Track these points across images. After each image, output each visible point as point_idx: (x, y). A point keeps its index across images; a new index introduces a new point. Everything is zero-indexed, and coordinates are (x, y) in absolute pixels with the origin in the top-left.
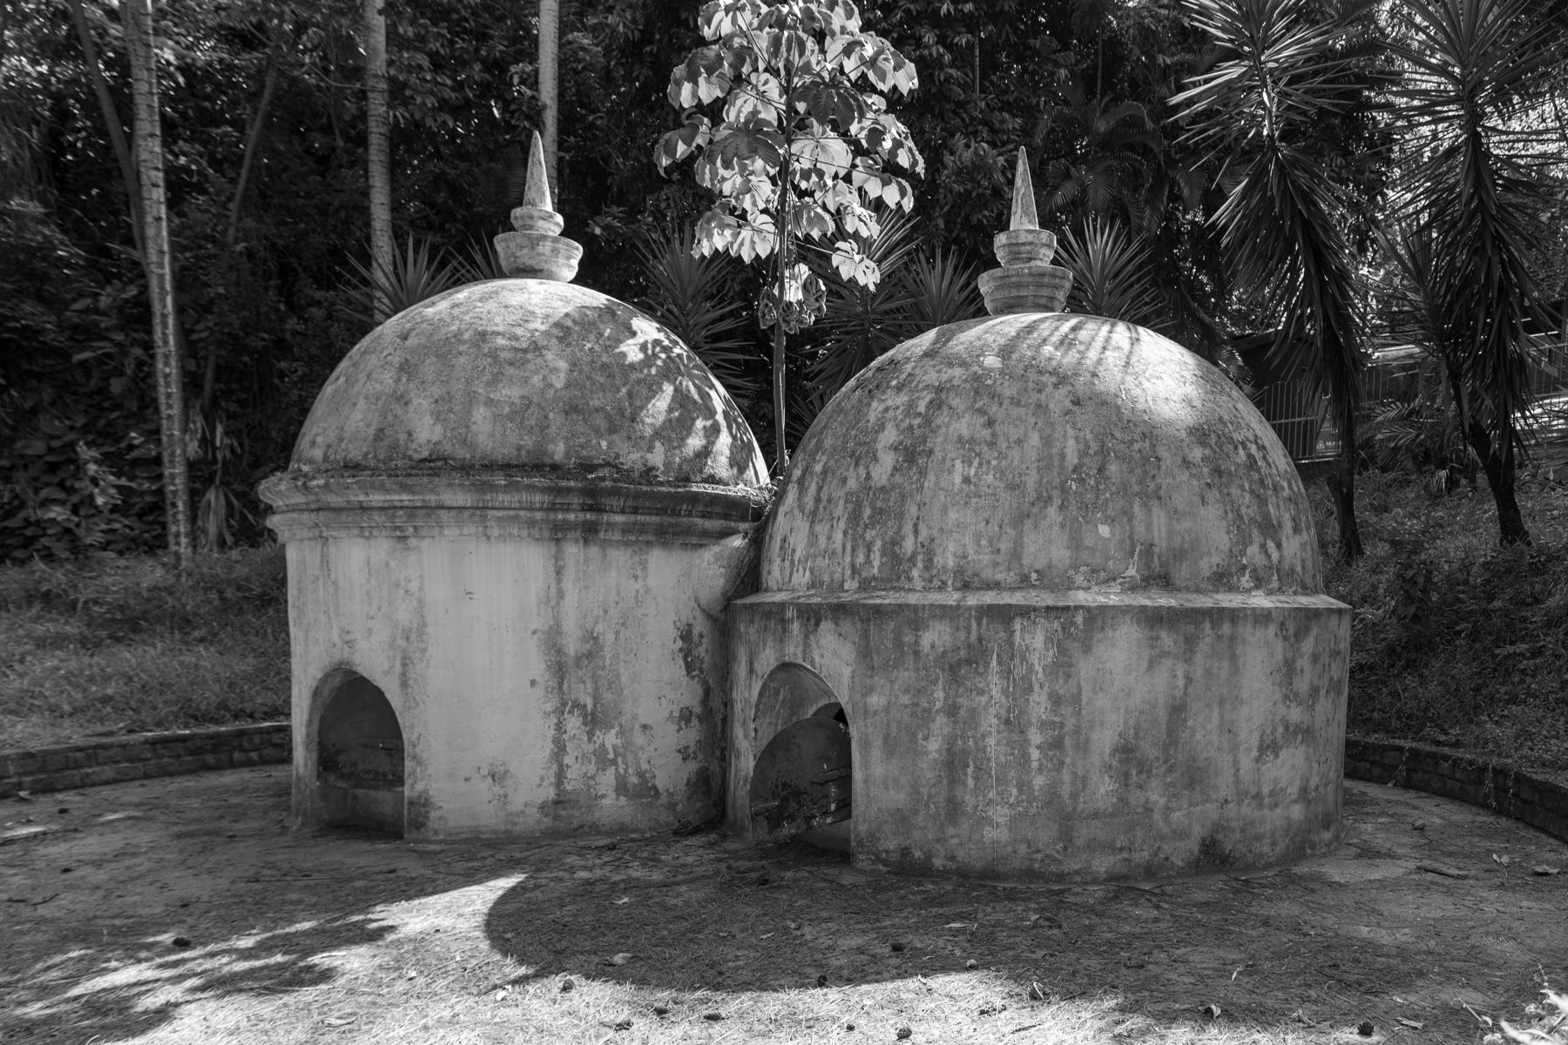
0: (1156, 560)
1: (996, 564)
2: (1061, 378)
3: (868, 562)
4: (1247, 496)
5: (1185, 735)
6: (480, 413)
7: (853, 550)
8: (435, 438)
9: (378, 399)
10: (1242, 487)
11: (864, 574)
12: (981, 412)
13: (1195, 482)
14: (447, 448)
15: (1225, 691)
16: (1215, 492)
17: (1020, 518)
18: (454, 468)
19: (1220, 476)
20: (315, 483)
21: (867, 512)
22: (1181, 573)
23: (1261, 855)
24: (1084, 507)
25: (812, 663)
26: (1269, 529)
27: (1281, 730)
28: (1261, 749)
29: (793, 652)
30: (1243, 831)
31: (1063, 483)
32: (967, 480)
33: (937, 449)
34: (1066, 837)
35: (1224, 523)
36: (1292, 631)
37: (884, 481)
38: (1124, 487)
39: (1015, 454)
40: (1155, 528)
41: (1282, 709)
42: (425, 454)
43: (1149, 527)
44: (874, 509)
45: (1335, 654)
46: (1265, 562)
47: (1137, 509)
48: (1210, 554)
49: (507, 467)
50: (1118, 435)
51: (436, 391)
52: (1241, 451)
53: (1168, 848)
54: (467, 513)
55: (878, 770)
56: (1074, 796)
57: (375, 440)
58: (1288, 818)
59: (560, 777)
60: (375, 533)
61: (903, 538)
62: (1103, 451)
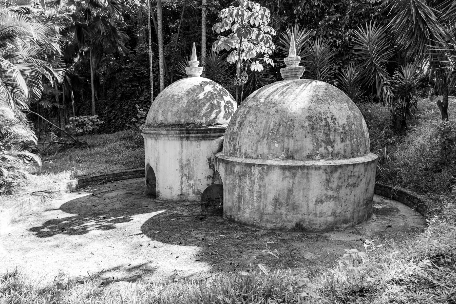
1: (252, 152)
2: (275, 105)
4: (322, 134)
5: (292, 197)
6: (170, 114)
12: (255, 114)
13: (304, 132)
14: (163, 122)
15: (305, 187)
16: (310, 134)
17: (258, 141)
22: (297, 156)
23: (315, 229)
24: (272, 139)
30: (309, 222)
31: (268, 133)
32: (249, 132)
34: (261, 218)
35: (312, 142)
39: (260, 125)
42: (160, 123)
43: (288, 144)
48: (306, 151)
50: (284, 120)
51: (163, 109)
53: (286, 224)
56: (263, 209)
59: (182, 189)
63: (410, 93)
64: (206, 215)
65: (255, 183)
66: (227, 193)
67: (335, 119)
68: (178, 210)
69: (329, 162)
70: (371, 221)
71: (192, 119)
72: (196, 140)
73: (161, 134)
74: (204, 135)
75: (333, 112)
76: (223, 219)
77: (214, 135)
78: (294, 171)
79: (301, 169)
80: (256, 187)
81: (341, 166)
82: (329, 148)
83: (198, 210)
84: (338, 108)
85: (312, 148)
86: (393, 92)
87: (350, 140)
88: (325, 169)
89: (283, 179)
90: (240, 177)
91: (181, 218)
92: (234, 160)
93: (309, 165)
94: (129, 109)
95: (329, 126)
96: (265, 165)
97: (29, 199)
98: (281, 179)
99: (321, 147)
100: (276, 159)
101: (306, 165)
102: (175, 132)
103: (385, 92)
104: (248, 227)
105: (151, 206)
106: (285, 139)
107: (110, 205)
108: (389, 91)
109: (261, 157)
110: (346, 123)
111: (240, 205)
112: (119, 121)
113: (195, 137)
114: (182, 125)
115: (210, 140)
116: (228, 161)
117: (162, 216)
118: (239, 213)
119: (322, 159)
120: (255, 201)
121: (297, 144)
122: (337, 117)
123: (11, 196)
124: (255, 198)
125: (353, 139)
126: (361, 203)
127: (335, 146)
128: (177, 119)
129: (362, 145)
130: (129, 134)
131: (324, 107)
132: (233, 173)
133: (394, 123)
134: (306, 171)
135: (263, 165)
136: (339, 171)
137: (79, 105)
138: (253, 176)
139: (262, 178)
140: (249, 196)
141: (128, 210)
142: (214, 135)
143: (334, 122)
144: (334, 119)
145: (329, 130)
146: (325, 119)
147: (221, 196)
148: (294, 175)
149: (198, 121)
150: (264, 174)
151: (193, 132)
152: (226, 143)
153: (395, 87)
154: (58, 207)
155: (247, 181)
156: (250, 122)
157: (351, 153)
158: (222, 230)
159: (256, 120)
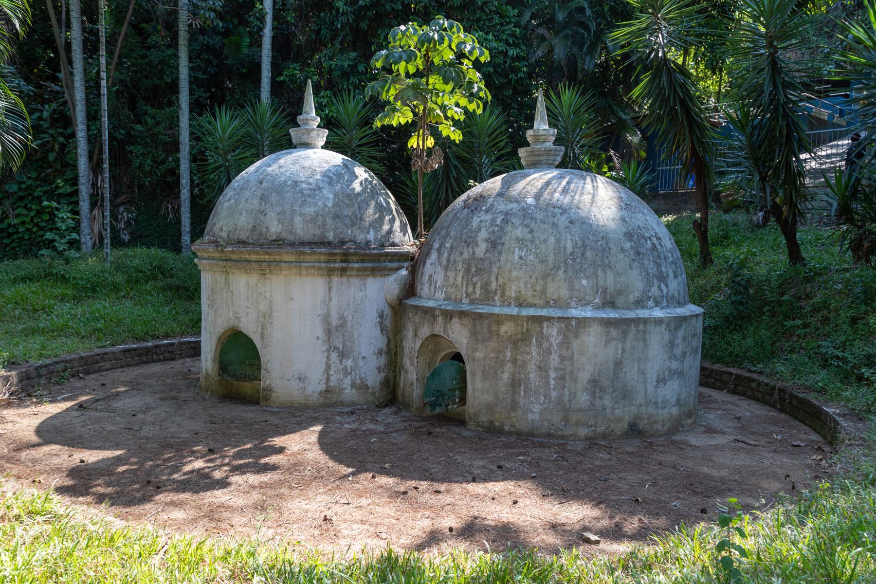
3: (474, 292)
4: (652, 264)
6: (298, 219)
7: (467, 286)
8: (279, 231)
9: (252, 212)
10: (649, 260)
11: (472, 297)
13: (627, 259)
14: (284, 235)
16: (636, 263)
18: (288, 245)
19: (639, 255)
20: (227, 249)
21: (474, 269)
25: (448, 336)
26: (662, 278)
29: (438, 329)
33: (506, 243)
35: (641, 277)
36: (673, 327)
37: (481, 256)
41: (668, 363)
42: (274, 238)
44: (477, 268)
45: (694, 335)
46: (660, 294)
49: (310, 244)
51: (278, 209)
52: (649, 242)
54: (293, 264)
57: (252, 231)
60: (252, 272)
61: (491, 282)
71: (349, 232)
72: (358, 276)
74: (376, 265)
78: (625, 327)
79: (635, 325)
89: (606, 343)
90: (515, 343)
96: (572, 318)
98: (603, 343)
106: (600, 272)
109: (558, 303)
111: (517, 397)
113: (359, 270)
114: (329, 243)
115: (382, 275)
120: (552, 387)
121: (619, 280)
124: (552, 382)
128: (318, 232)
132: (495, 338)
135: (568, 318)
138: (547, 340)
139: (565, 344)
148: (625, 334)
149: (361, 237)
151: (355, 258)
155: (534, 350)
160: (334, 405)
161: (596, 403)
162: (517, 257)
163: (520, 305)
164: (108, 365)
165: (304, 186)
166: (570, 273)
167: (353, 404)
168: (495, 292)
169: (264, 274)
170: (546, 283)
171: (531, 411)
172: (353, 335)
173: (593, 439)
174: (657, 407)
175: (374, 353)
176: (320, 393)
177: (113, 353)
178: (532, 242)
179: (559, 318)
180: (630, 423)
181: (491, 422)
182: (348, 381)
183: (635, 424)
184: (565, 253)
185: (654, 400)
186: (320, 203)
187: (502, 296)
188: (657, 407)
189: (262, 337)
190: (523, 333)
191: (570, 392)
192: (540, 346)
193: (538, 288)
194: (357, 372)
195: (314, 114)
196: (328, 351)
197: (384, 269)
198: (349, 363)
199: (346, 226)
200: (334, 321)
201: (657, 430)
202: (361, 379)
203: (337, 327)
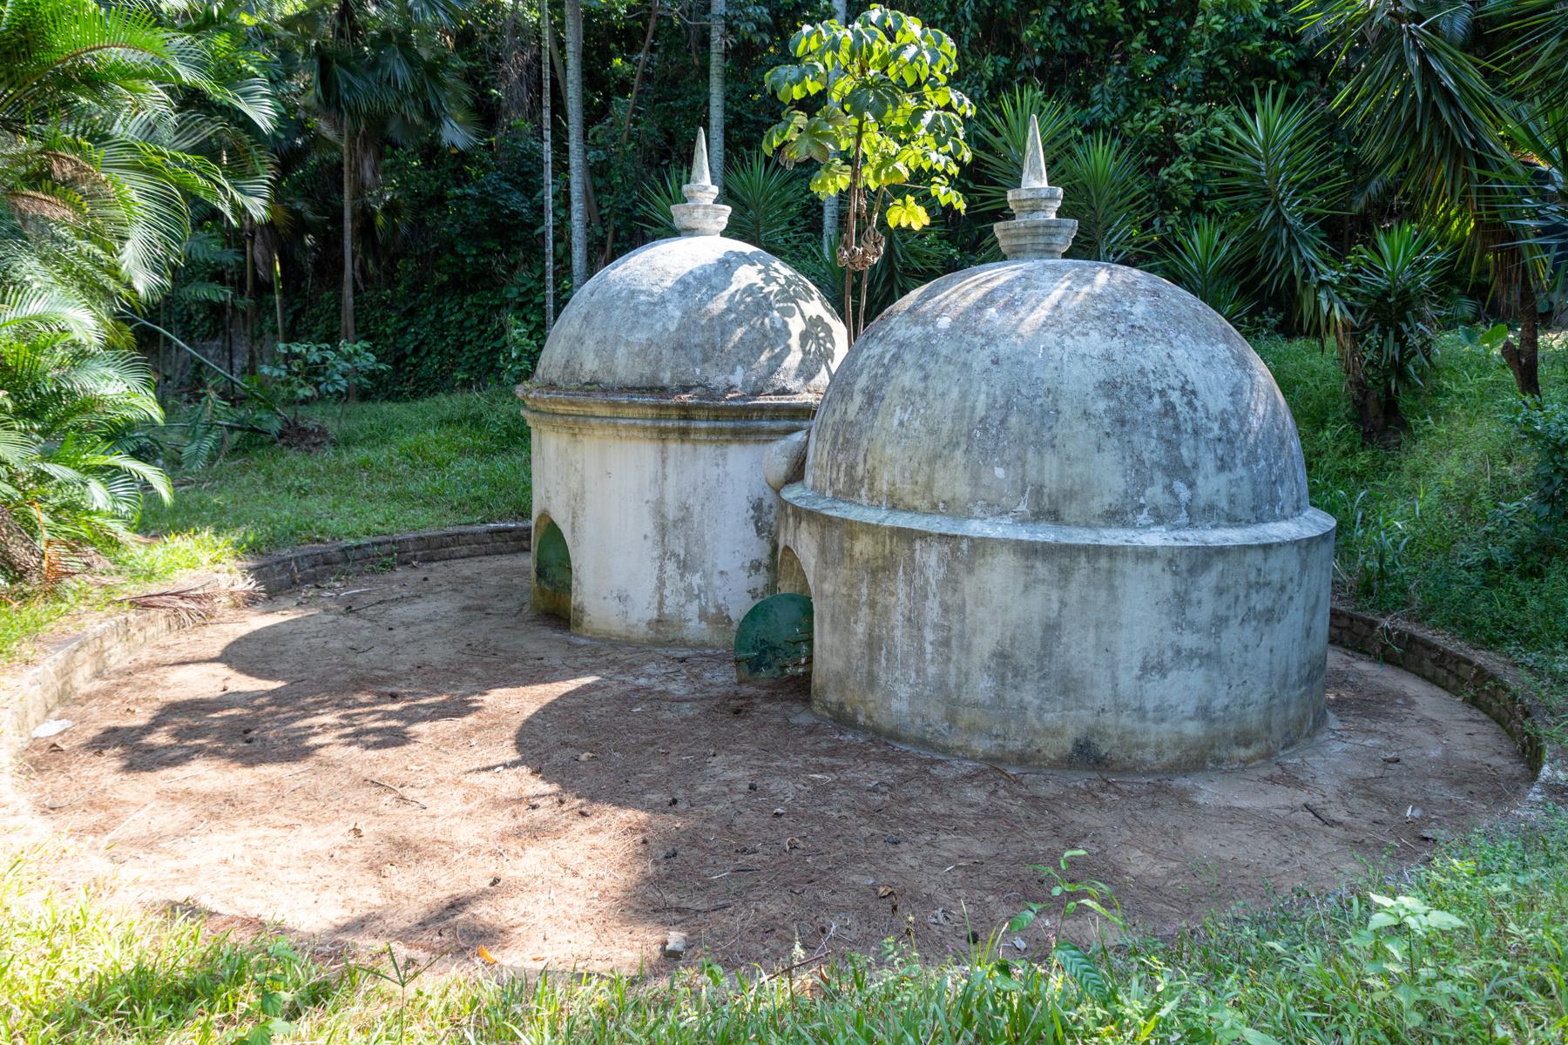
0: (1046, 499)
10: (1148, 435)
14: (600, 376)
19: (1123, 425)
21: (841, 440)
22: (1070, 511)
27: (1169, 654)
28: (1145, 669)
38: (1021, 437)
40: (1046, 472)
47: (1030, 455)
48: (1101, 495)
51: (599, 335)
55: (828, 640)
58: (1180, 733)
62: (1008, 406)
63: (1409, 313)
64: (750, 697)
65: (926, 597)
66: (827, 627)
67: (1194, 393)
68: (650, 676)
69: (1183, 534)
70: (1325, 737)
71: (698, 371)
72: (711, 441)
73: (593, 416)
74: (739, 424)
75: (1185, 371)
76: (814, 714)
77: (774, 425)
78: (1066, 561)
79: (1088, 557)
80: (932, 610)
81: (1222, 551)
82: (1179, 486)
83: (722, 678)
84: (1201, 359)
85: (1123, 487)
86: (1351, 308)
87: (1247, 464)
88: (1171, 558)
89: (1026, 588)
90: (874, 573)
91: (665, 705)
92: (851, 517)
93: (1115, 543)
94: (467, 324)
95: (1175, 417)
96: (962, 537)
97: (127, 621)
98: (1020, 588)
99: (1152, 484)
100: (998, 520)
101: (1103, 542)
102: (641, 411)
103: (1325, 306)
104: (904, 748)
105: (555, 658)
107: (410, 649)
108: (1336, 306)
109: (950, 508)
110: (1231, 408)
112: (433, 363)
113: (710, 432)
114: (663, 389)
116: (830, 519)
117: (599, 694)
118: (870, 697)
119: (1158, 523)
120: (929, 657)
122: (1200, 387)
123: (64, 606)
124: (929, 649)
125: (1257, 461)
126: (1294, 678)
127: (1200, 481)
128: (647, 371)
129: (1287, 484)
130: (468, 407)
131: (1156, 351)
132: (847, 560)
133: (1360, 407)
134: (1103, 563)
136: (1219, 566)
137: (298, 306)
138: (921, 573)
139: (951, 582)
140: (906, 640)
141: (475, 670)
142: (774, 425)
143: (1190, 404)
144: (1190, 393)
145: (1177, 428)
146: (1162, 393)
147: (806, 636)
148: (1065, 574)
149: (720, 378)
150: (959, 567)
152: (817, 454)
153: (1354, 295)
154: (216, 653)
155: (901, 589)
156: (903, 390)
157: (1253, 509)
158: (816, 754)
159: (926, 387)
160: (671, 643)
161: (1007, 696)
162: (896, 422)
163: (894, 507)
164: (465, 550)
165: (643, 298)
166: (975, 454)
167: (703, 645)
168: (862, 481)
169: (574, 435)
170: (933, 471)
171: (896, 695)
172: (703, 536)
173: (1000, 760)
174: (1143, 718)
175: (743, 567)
176: (649, 623)
177: (474, 534)
178: (923, 395)
179: (941, 535)
180: (1077, 741)
181: (841, 705)
182: (693, 609)
183: (1088, 744)
184: (971, 418)
185: (1135, 704)
186: (658, 326)
187: (870, 490)
188: (1143, 718)
189: (573, 531)
190: (884, 557)
191: (959, 669)
192: (910, 582)
193: (920, 480)
194: (710, 595)
195: (706, 180)
196: (662, 558)
197: (758, 431)
198: (696, 580)
199: (694, 362)
200: (672, 513)
201: (1143, 762)
202: (718, 607)
203: (675, 523)
